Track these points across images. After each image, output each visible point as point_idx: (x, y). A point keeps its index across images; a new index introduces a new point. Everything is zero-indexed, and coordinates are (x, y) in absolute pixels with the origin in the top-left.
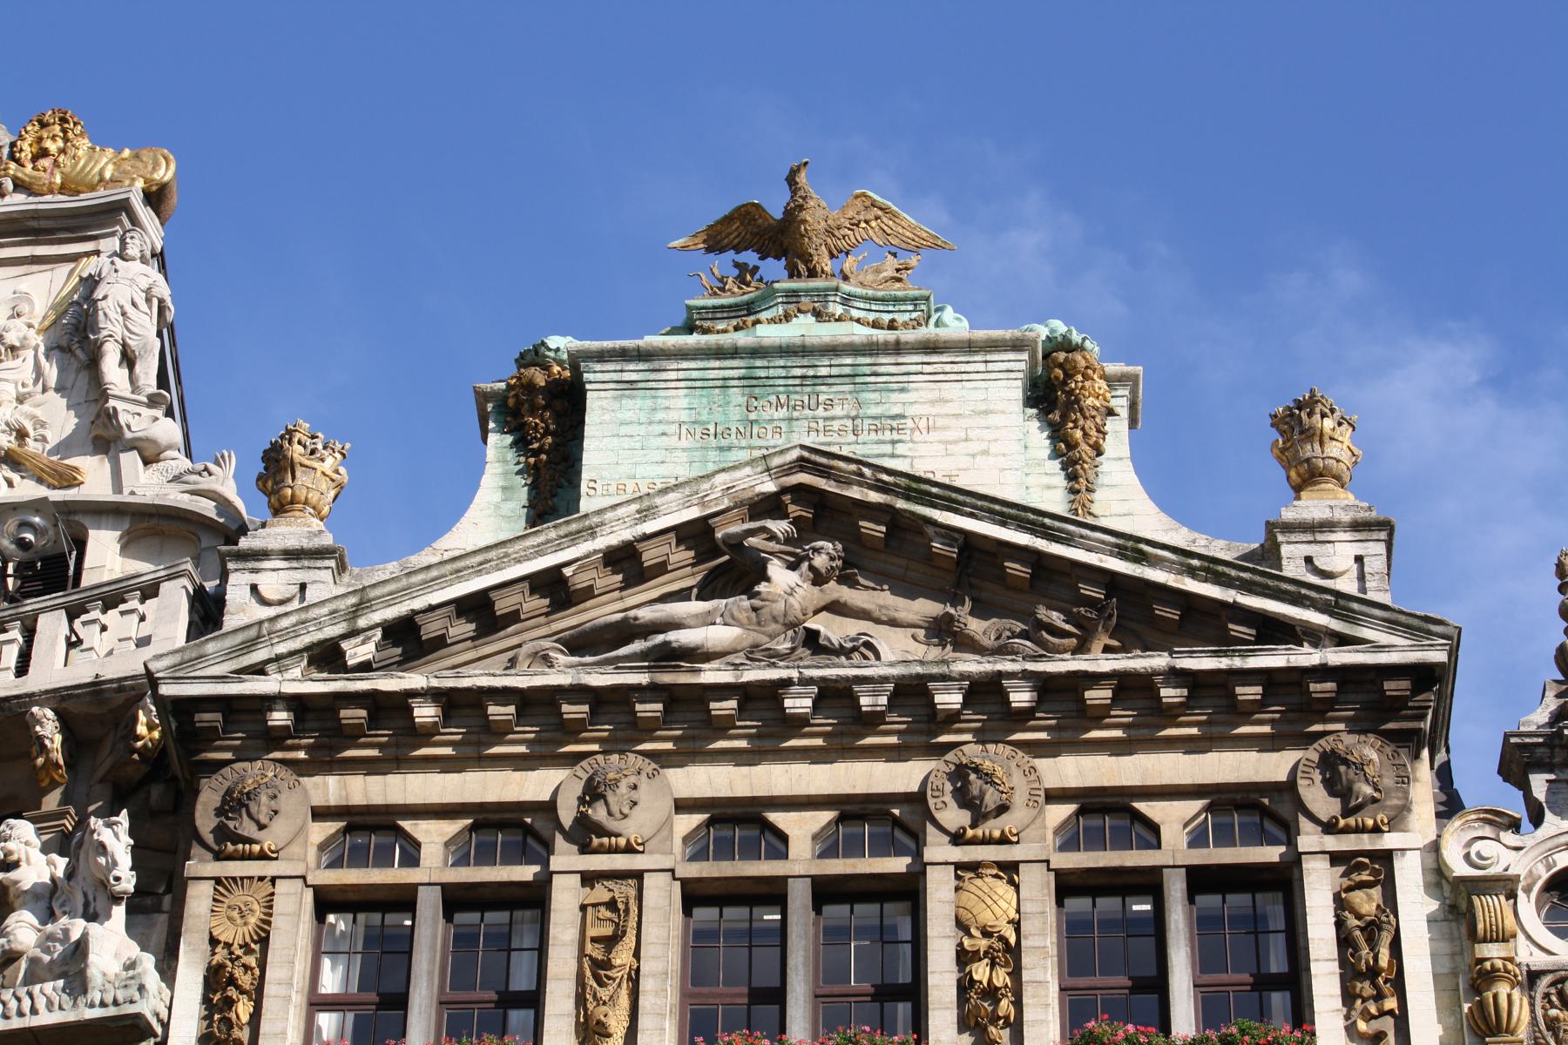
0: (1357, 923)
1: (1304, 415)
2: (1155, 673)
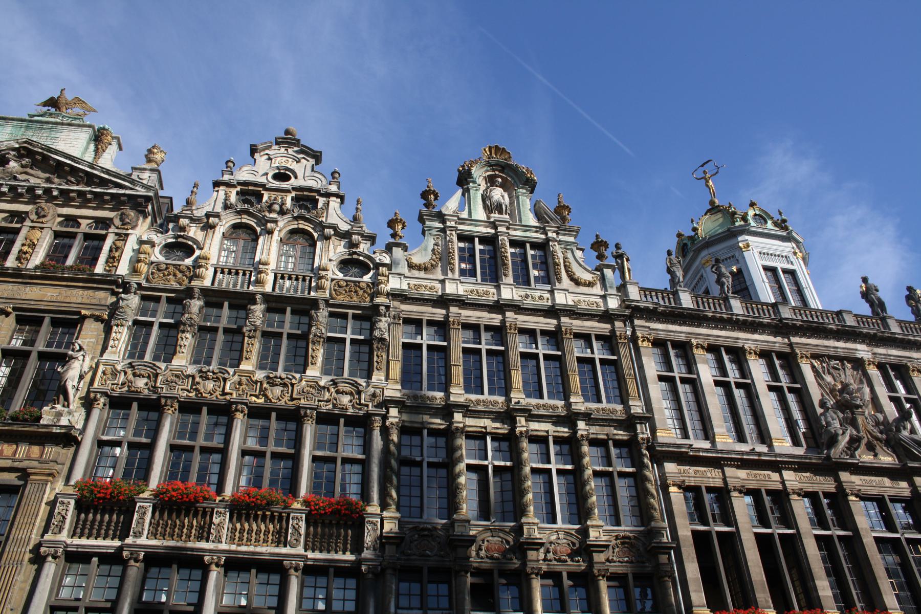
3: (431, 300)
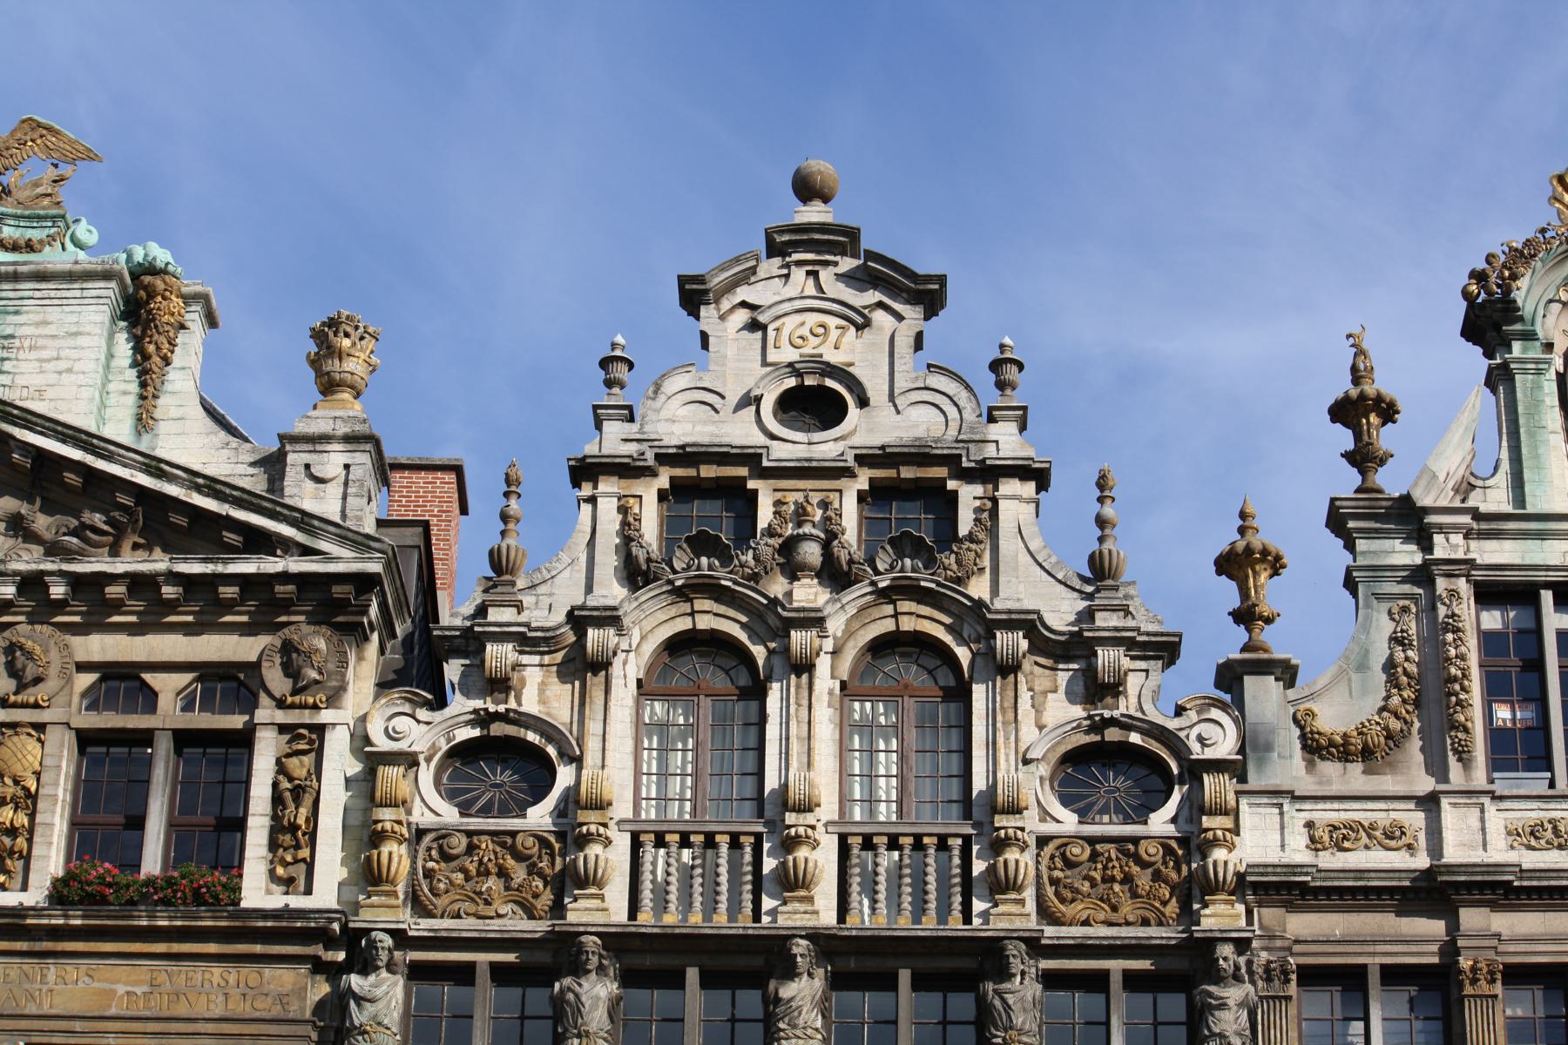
0: (289, 786)
1: (331, 334)
2: (158, 574)
3: (1390, 891)
